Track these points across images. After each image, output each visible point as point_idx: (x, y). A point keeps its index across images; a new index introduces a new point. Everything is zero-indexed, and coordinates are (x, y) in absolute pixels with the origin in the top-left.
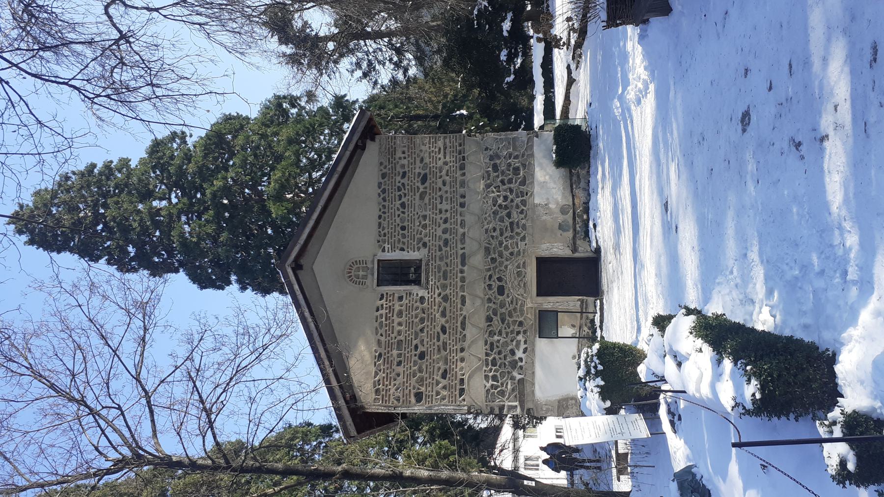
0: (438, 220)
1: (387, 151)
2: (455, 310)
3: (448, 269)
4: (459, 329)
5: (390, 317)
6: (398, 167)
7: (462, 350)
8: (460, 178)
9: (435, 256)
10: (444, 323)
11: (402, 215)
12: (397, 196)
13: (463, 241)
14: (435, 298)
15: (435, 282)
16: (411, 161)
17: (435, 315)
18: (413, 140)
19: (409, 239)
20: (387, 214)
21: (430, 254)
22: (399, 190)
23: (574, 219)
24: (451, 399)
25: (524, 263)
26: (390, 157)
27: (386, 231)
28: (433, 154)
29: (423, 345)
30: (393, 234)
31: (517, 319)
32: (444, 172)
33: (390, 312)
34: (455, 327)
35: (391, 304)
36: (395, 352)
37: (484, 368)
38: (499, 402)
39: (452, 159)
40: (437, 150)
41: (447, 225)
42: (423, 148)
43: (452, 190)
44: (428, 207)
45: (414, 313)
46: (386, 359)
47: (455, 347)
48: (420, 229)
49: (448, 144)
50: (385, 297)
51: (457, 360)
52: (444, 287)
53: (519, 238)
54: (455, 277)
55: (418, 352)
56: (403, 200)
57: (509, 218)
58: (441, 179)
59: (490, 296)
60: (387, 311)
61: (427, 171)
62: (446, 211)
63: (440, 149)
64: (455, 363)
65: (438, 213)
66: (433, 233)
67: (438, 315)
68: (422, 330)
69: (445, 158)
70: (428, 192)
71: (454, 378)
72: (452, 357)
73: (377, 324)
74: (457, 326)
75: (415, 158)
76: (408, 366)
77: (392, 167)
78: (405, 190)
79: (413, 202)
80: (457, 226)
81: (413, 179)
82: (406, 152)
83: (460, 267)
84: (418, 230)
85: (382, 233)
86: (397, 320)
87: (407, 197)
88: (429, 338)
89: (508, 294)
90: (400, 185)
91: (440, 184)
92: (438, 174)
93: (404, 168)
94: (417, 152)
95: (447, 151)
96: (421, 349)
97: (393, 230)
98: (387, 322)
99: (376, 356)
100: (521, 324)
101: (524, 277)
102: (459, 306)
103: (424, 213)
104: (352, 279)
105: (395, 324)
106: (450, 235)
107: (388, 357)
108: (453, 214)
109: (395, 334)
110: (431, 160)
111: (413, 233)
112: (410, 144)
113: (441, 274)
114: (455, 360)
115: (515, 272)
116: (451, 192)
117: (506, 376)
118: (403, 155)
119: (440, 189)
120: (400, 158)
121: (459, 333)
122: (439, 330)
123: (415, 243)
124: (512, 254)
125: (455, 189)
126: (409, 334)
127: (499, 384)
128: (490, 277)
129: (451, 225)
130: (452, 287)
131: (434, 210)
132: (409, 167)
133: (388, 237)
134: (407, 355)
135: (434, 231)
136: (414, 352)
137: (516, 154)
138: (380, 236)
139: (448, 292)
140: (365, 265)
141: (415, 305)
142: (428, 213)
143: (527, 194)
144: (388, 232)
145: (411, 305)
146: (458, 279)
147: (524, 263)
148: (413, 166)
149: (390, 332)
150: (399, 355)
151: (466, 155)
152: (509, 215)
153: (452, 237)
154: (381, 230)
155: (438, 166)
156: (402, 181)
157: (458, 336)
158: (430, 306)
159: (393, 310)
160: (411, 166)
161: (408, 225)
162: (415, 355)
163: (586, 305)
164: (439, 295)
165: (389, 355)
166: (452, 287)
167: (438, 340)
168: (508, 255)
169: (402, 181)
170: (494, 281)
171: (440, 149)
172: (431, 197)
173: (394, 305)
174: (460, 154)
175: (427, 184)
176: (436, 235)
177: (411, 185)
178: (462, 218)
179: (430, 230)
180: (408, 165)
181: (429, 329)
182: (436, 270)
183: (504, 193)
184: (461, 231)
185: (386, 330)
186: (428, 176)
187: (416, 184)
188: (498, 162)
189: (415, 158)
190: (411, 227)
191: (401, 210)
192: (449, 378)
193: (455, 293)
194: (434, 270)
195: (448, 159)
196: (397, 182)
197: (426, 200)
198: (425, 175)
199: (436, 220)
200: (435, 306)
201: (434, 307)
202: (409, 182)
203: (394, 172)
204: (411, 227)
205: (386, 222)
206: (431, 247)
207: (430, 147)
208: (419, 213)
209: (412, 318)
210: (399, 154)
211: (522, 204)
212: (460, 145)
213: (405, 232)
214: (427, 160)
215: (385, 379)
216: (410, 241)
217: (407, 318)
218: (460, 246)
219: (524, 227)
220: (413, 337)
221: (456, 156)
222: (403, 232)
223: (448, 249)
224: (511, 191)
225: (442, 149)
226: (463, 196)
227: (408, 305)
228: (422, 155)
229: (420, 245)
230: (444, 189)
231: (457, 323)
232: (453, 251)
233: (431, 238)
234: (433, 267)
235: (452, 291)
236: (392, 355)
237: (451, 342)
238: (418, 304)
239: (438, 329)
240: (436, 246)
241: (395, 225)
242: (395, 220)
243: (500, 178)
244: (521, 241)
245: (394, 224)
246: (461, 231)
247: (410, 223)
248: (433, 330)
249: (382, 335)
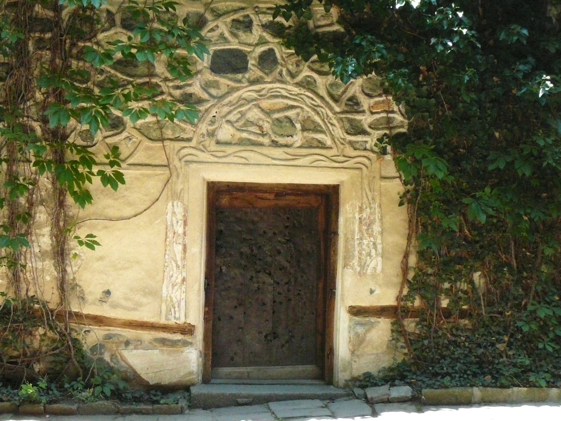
25: (322, 145)
59: (211, 25)
89: (216, 85)
115: (291, 113)
124: (353, 103)
147: (322, 145)
163: (174, 344)
168: (349, 94)
170: (262, 42)
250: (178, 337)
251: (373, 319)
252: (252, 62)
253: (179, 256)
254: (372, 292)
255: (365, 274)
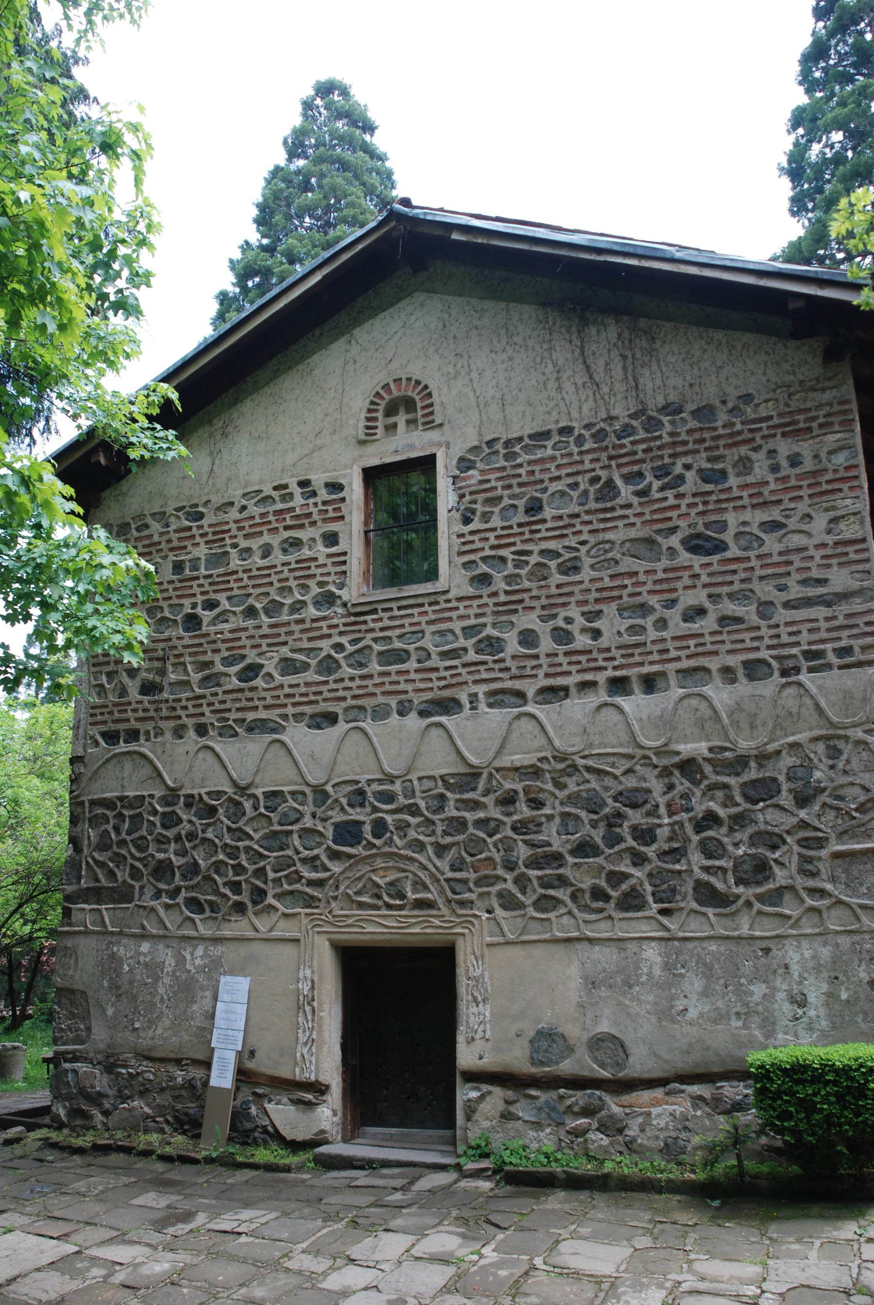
0: (563, 613)
1: (794, 405)
2: (298, 699)
3: (412, 664)
4: (250, 716)
5: (285, 519)
6: (743, 450)
7: (202, 730)
8: (713, 664)
9: (450, 619)
10: (264, 671)
11: (575, 494)
12: (636, 468)
13: (497, 698)
14: (329, 636)
15: (372, 630)
16: (766, 491)
17: (285, 643)
18: (845, 486)
19: (500, 532)
20: (576, 450)
21: (454, 604)
22: (662, 472)
23: (578, 1083)
24: (98, 711)
26: (776, 421)
27: (523, 458)
28: (797, 564)
29: (215, 625)
30: (514, 482)
31: (270, 884)
32: (731, 608)
33: (297, 517)
34: (257, 703)
35: (315, 517)
36: (201, 551)
37: (158, 794)
38: (89, 837)
39: (783, 630)
40: (815, 574)
41: (547, 644)
42: (820, 522)
43: (670, 645)
44: (605, 574)
45: (292, 583)
46: (188, 534)
47: (206, 710)
48: (534, 559)
49: (844, 608)
50: (334, 497)
51: (179, 717)
52: (359, 659)
53: (510, 886)
54: (388, 687)
55: (199, 610)
56: (626, 491)
57: (573, 852)
58: (707, 604)
60: (298, 511)
61: (734, 551)
62: (596, 634)
63: (822, 582)
64: (174, 714)
65: (585, 609)
66: (521, 601)
67: (285, 651)
68: (251, 612)
69: (787, 605)
70: (660, 566)
71: (141, 714)
72: (184, 703)
73: (268, 490)
74: (256, 708)
75: (779, 502)
76: (172, 593)
77: (739, 433)
78: (662, 489)
79: (620, 523)
80: (547, 675)
81: (701, 508)
82: (797, 470)
83: (417, 699)
84: (528, 553)
85: (517, 449)
86: (274, 541)
87: (635, 500)
88: (230, 636)
90: (678, 469)
91: (689, 599)
92: (726, 589)
93: (738, 475)
94: (803, 507)
95: (820, 612)
96: (207, 616)
97: (524, 479)
98: (271, 518)
99: (196, 505)
100: (259, 894)
101: (389, 907)
102: (308, 710)
103: (587, 561)
104: (382, 398)
105: (266, 538)
106: (514, 657)
107: (193, 537)
108: (583, 658)
109: (244, 544)
110: (776, 559)
111: (517, 539)
112: (830, 476)
113: (398, 645)
114: (179, 712)
116: (663, 640)
117: (138, 855)
118: (784, 463)
119: (671, 603)
120: (772, 453)
121: (239, 715)
122: (248, 661)
123: (488, 552)
125: (673, 654)
126: (241, 580)
127: (124, 836)
128: (389, 797)
129: (548, 655)
130: (358, 682)
131: (594, 595)
132: (742, 487)
133: (504, 468)
134: (195, 583)
135: (528, 603)
136: (199, 599)
137: (821, 865)
138: (508, 443)
139: (347, 671)
140: (421, 421)
141: (311, 583)
142: (586, 574)
143: (662, 912)
144: (520, 466)
145: (313, 571)
146: (381, 699)
148: (746, 501)
149: (247, 530)
150: (195, 564)
151: (803, 677)
152: (584, 849)
153: (509, 663)
154: (527, 441)
155: (756, 586)
156: (690, 476)
157: (233, 715)
158: (307, 625)
159: (302, 526)
160: (745, 494)
161: (544, 521)
162: (194, 606)
164: (339, 647)
165: (198, 539)
166: (358, 682)
167: (228, 662)
169: (690, 476)
171: (822, 582)
172: (642, 578)
173: (313, 524)
174: (809, 655)
175: (685, 557)
176: (516, 611)
177: (678, 507)
178: (573, 690)
179: (529, 590)
180: (751, 485)
181: (251, 632)
182: (408, 629)
183: (663, 833)
184: (530, 688)
185: (253, 518)
186: (716, 558)
187: (683, 523)
188: (785, 799)
189: (779, 502)
190: (539, 531)
191: (592, 490)
192: (141, 702)
193: (341, 693)
194: (406, 621)
195: (782, 615)
196: (689, 460)
197: (628, 564)
198: (721, 547)
199: (564, 605)
200: (310, 639)
201: (305, 636)
202: (688, 500)
203: (722, 442)
204: (539, 531)
205: (549, 452)
206: (475, 603)
207: (824, 545)
208: (584, 549)
209: (280, 581)
210: (784, 448)
211: (625, 895)
212: (843, 652)
213: (521, 517)
214: (772, 544)
215: (147, 542)
216: (491, 535)
217: (279, 569)
218: (481, 690)
219: (545, 903)
220: (236, 592)
221: (798, 644)
222: (521, 510)
223: (472, 656)
224: (675, 854)
225: (820, 591)
226: (650, 684)
227: (313, 564)
228: (792, 523)
229: (484, 568)
230: (674, 616)
231: (266, 707)
232: (463, 671)
233: (502, 598)
234: (416, 619)
235: (347, 683)
236: (197, 545)
237: (220, 697)
238: (316, 590)
239: (252, 657)
240: (477, 616)
241: (542, 481)
242: (558, 478)
243: (722, 812)
244: (500, 895)
245: (546, 476)
246: (530, 688)
247: (549, 525)
248: (249, 643)
249: (244, 508)
250: (309, 1097)
251: (485, 1088)
252: (367, 829)
253: (310, 1018)
254: (481, 1058)
255: (473, 1039)
